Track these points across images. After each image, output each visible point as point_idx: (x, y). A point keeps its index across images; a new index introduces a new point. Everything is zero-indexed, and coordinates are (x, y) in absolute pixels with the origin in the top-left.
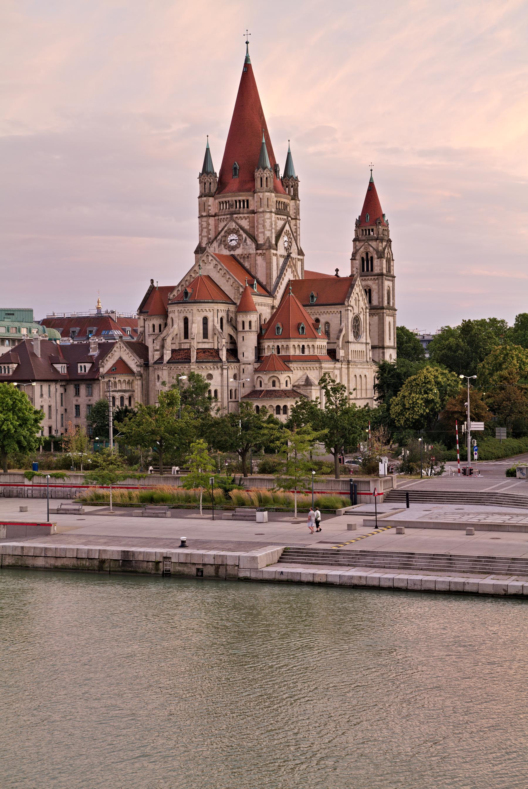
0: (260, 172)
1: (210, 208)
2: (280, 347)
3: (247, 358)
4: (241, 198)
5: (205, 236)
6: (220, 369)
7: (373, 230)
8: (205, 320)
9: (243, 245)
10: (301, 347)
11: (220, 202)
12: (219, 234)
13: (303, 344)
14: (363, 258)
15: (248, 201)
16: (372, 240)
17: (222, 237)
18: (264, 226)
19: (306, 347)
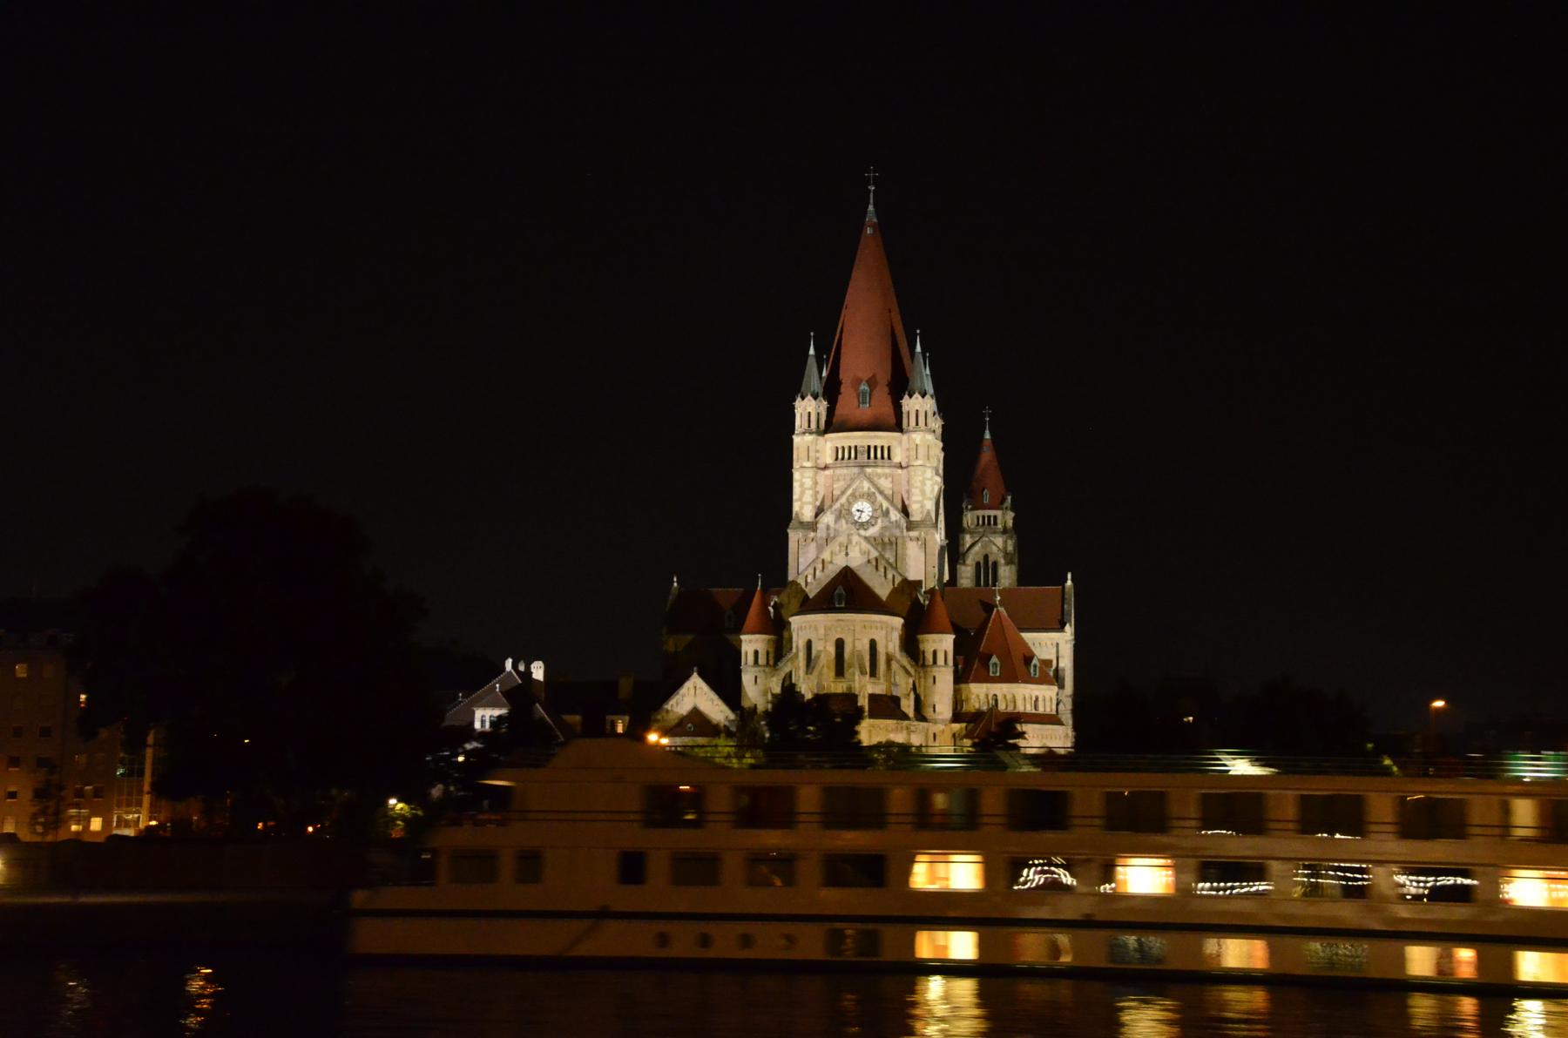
0: (917, 398)
1: (818, 455)
2: (999, 698)
3: (941, 713)
4: (879, 443)
5: (809, 503)
6: (905, 732)
7: (995, 517)
8: (873, 644)
9: (882, 522)
10: (1034, 699)
11: (837, 448)
12: (837, 499)
13: (1037, 693)
14: (978, 564)
15: (889, 448)
16: (995, 533)
17: (842, 505)
18: (923, 492)
19: (1040, 699)
